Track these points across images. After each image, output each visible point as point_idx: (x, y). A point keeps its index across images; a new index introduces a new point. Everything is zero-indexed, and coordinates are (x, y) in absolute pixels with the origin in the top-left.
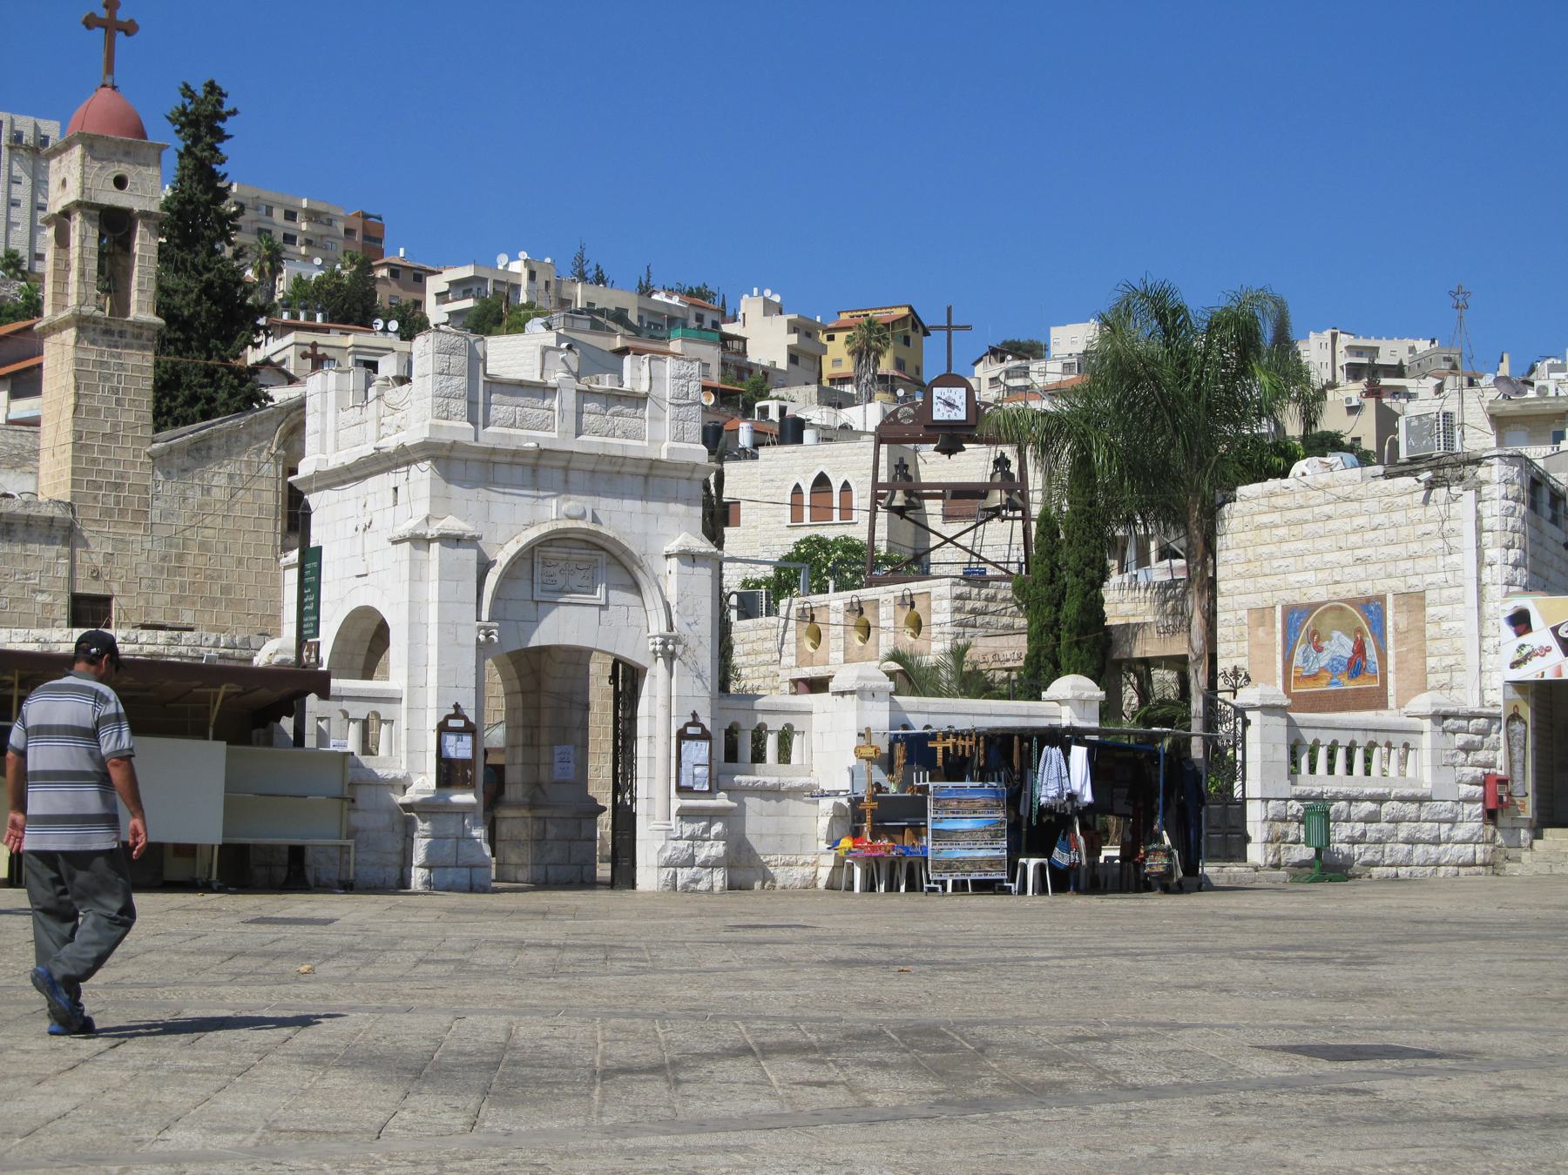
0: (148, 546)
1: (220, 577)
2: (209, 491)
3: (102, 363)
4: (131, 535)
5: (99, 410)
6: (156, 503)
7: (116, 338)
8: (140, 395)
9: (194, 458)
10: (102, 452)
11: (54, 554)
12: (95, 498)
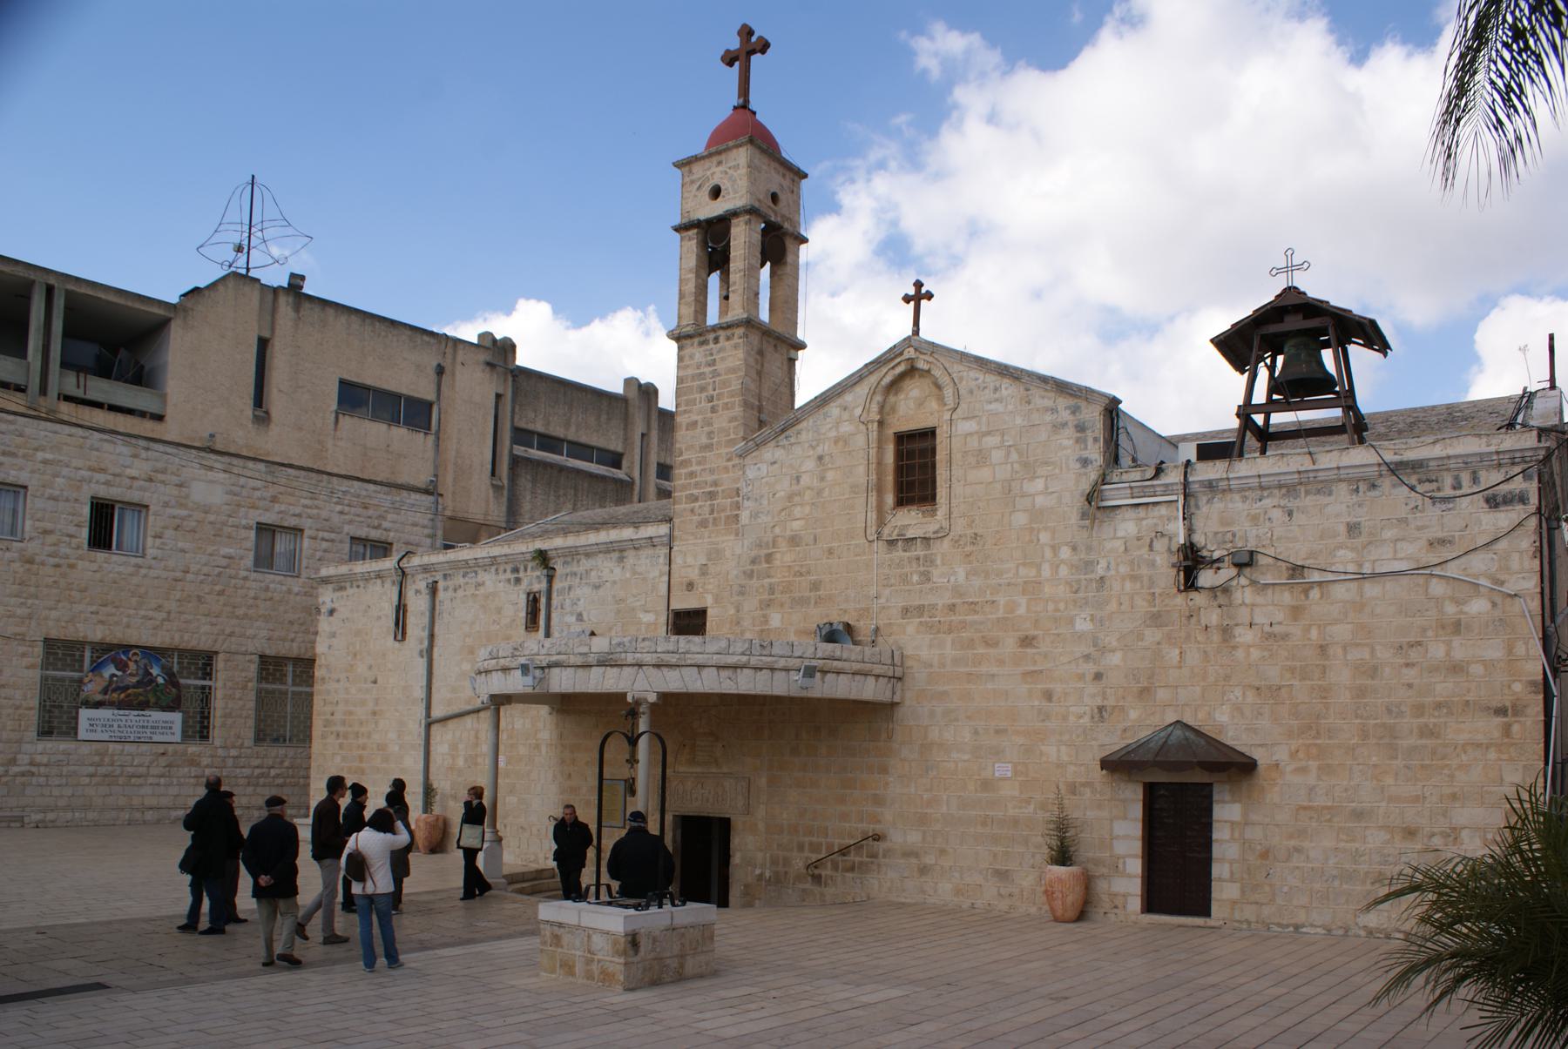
0: (738, 551)
1: (808, 573)
2: (798, 479)
3: (701, 374)
4: (723, 542)
5: (695, 423)
6: (746, 503)
7: (712, 345)
8: (733, 396)
9: (784, 447)
10: (699, 463)
11: (657, 574)
12: (692, 511)
